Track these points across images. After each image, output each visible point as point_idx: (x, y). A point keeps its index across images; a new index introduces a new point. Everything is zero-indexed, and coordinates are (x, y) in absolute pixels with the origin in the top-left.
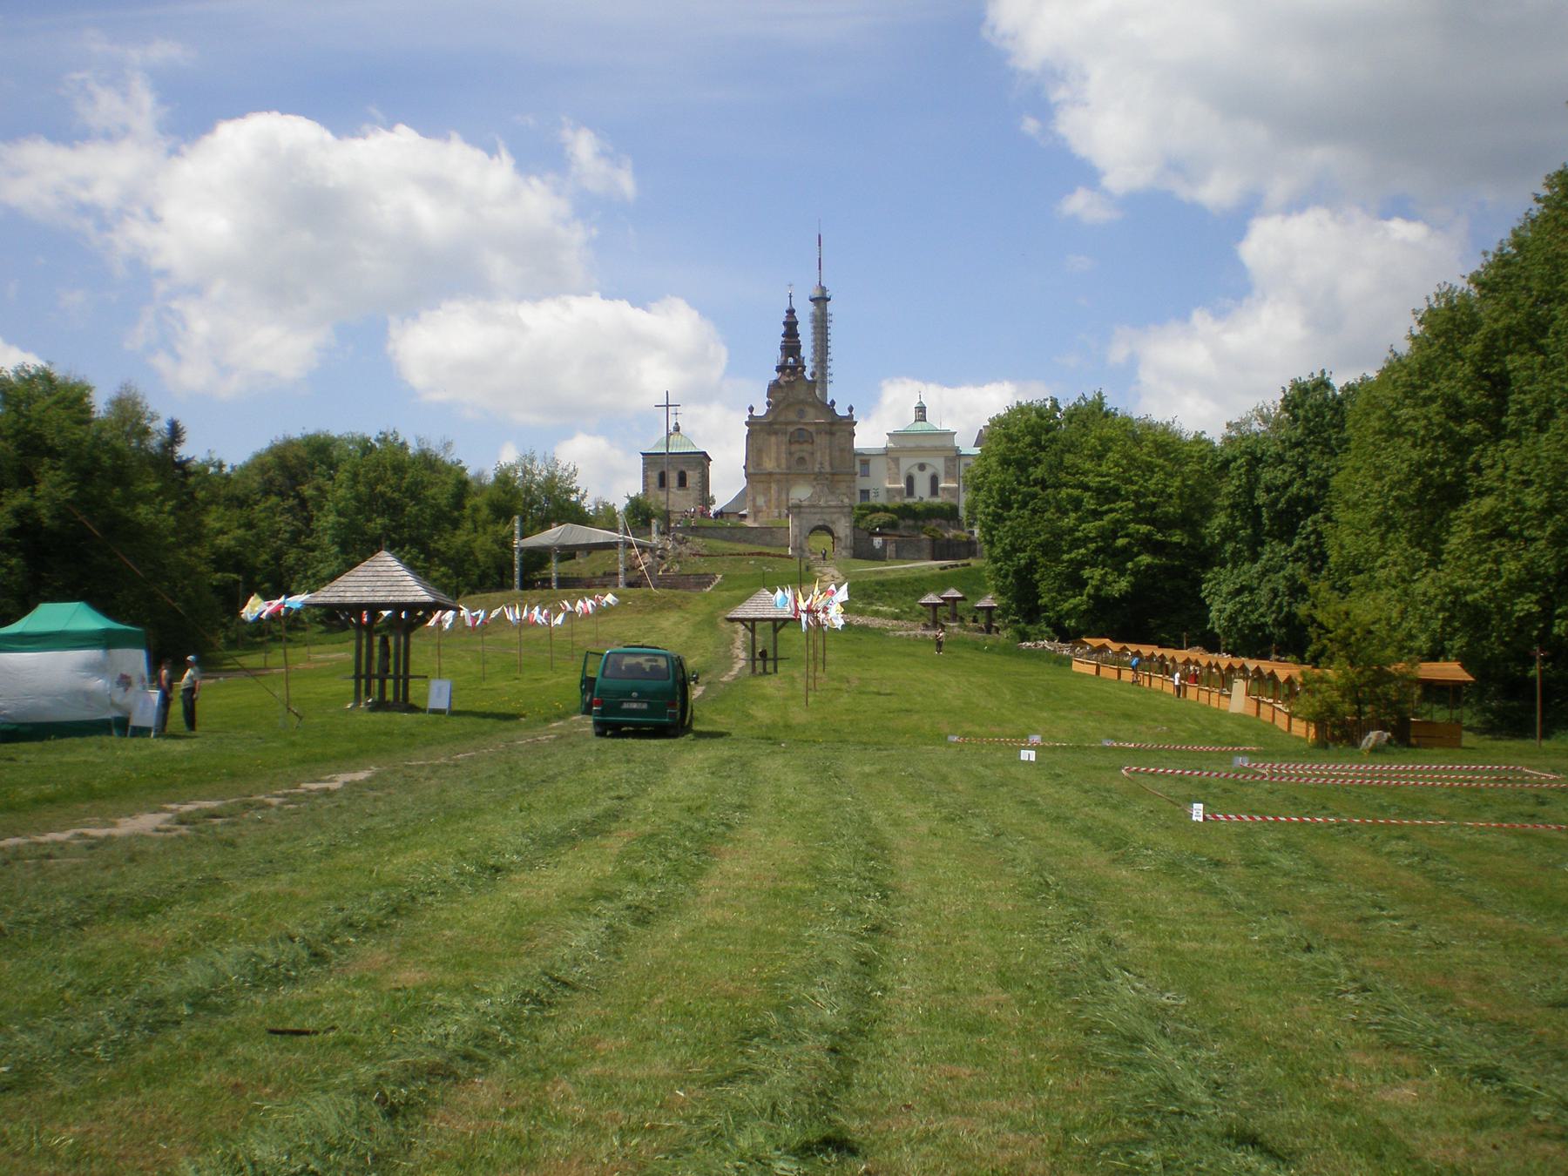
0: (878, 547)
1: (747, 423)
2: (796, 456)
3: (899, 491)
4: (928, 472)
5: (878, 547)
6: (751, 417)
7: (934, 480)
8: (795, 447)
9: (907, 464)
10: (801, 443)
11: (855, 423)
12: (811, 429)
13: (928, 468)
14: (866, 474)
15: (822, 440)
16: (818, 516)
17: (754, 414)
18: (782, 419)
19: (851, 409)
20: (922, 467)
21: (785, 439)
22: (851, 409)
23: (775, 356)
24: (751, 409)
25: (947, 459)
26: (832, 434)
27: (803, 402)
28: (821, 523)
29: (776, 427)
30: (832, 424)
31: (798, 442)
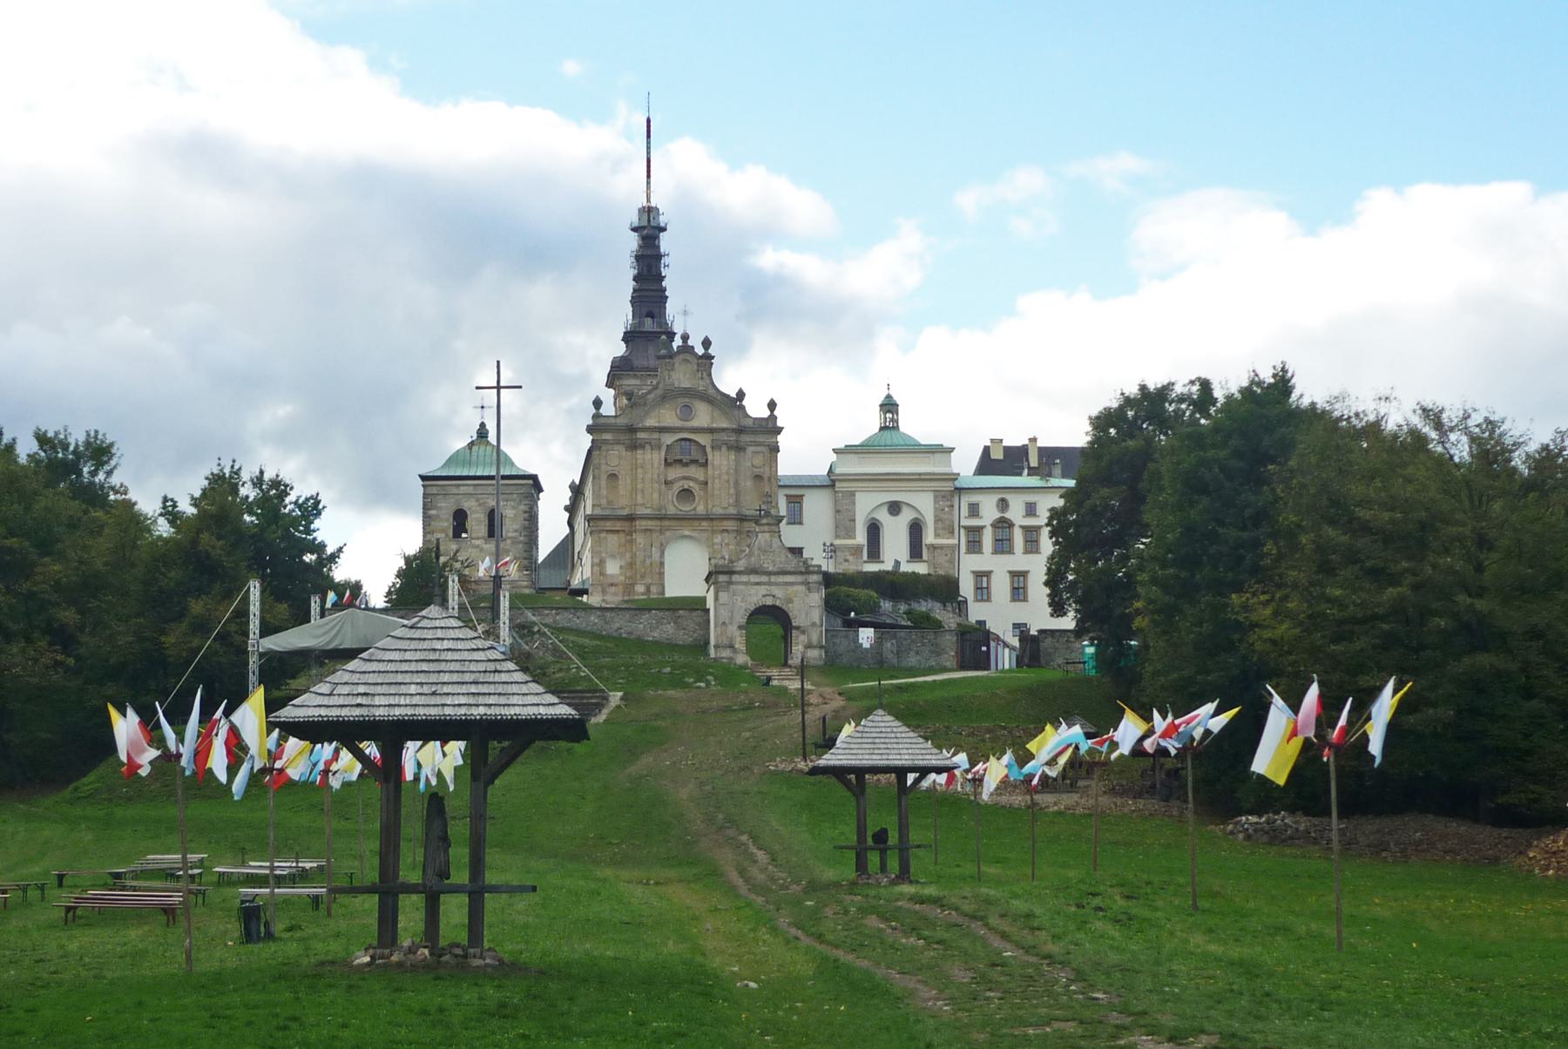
0: (866, 645)
1: (590, 430)
2: (677, 487)
3: (857, 550)
4: (906, 517)
5: (866, 645)
6: (596, 416)
7: (916, 529)
8: (675, 473)
9: (867, 504)
10: (686, 465)
11: (779, 430)
12: (703, 439)
13: (905, 510)
14: (796, 519)
15: (721, 461)
16: (763, 590)
18: (651, 422)
19: (772, 405)
20: (895, 508)
21: (657, 457)
22: (772, 405)
23: (623, 315)
25: (939, 496)
26: (739, 449)
27: (690, 393)
28: (769, 602)
29: (641, 435)
30: (740, 431)
31: (680, 461)
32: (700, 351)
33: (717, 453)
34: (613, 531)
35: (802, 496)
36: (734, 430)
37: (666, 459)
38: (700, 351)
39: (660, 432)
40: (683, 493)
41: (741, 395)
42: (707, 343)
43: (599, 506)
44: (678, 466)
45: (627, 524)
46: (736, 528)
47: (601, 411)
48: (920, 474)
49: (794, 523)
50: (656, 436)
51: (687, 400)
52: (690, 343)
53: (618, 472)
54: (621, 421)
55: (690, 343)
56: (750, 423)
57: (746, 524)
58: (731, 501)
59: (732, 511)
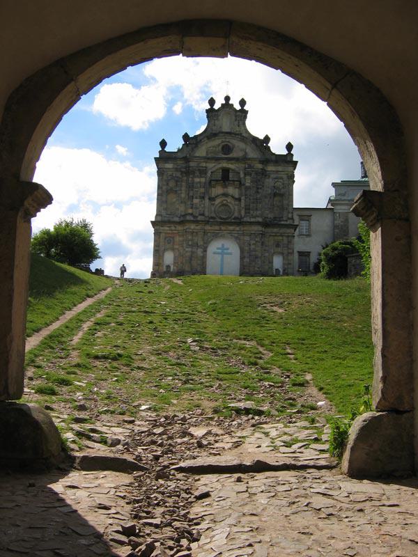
6: (162, 152)
17: (167, 149)
19: (289, 147)
22: (289, 147)
24: (163, 144)
29: (192, 164)
32: (238, 107)
33: (248, 177)
35: (310, 216)
38: (238, 107)
39: (206, 162)
41: (267, 139)
42: (243, 103)
43: (161, 215)
47: (165, 149)
52: (230, 102)
54: (180, 155)
55: (230, 102)
56: (273, 158)
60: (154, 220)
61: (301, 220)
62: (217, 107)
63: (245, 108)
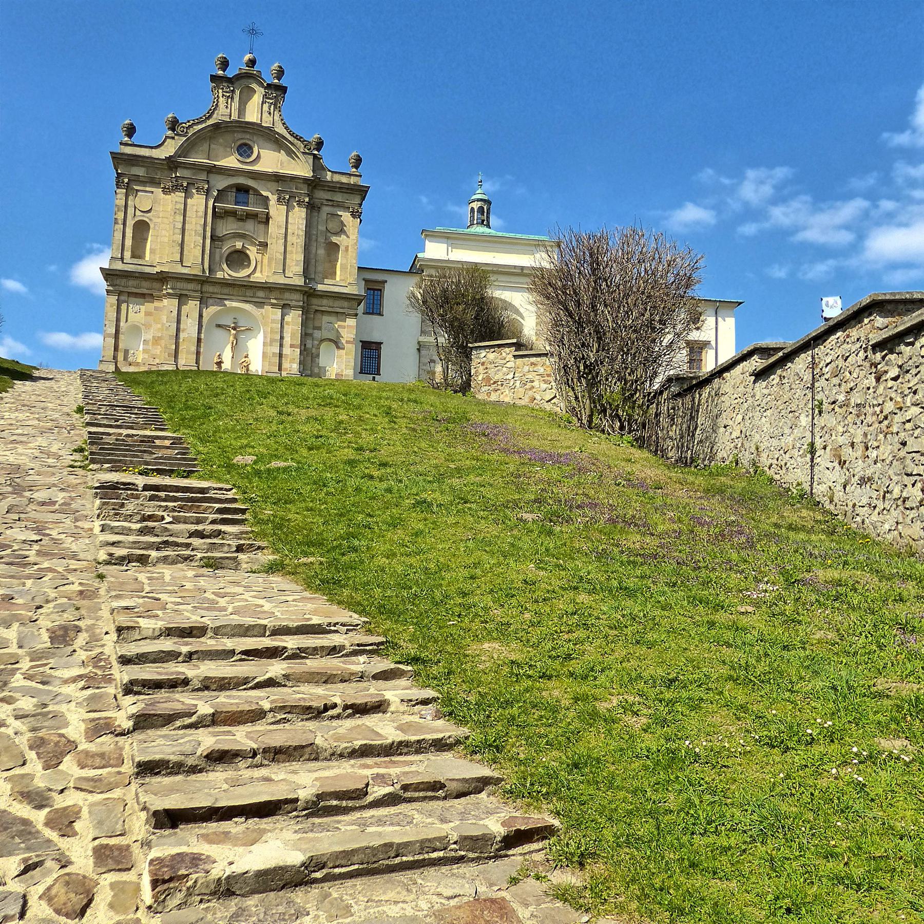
8: (227, 227)
34: (136, 295)
36: (305, 180)
37: (214, 207)
40: (235, 256)
44: (231, 219)
45: (156, 285)
46: (301, 303)
48: (522, 268)
49: (372, 314)
50: (203, 176)
51: (248, 136)
53: (151, 220)
57: (315, 301)
58: (300, 269)
59: (300, 281)
60: (107, 267)
61: (368, 289)
62: (231, 73)
63: (283, 82)
